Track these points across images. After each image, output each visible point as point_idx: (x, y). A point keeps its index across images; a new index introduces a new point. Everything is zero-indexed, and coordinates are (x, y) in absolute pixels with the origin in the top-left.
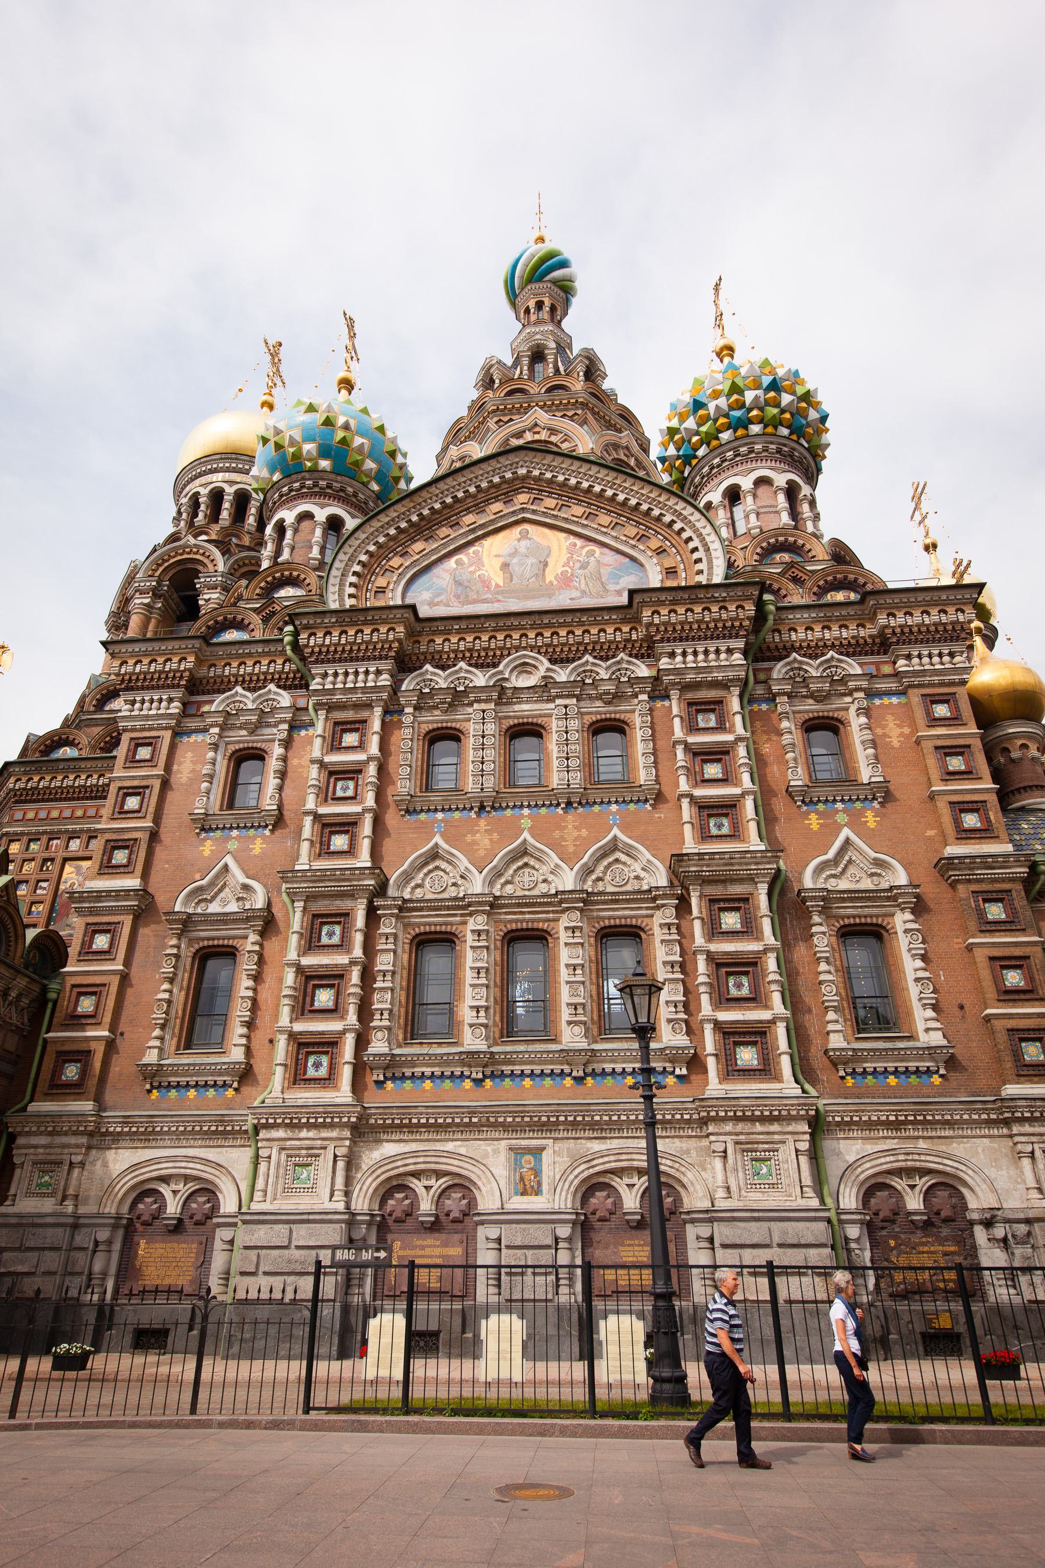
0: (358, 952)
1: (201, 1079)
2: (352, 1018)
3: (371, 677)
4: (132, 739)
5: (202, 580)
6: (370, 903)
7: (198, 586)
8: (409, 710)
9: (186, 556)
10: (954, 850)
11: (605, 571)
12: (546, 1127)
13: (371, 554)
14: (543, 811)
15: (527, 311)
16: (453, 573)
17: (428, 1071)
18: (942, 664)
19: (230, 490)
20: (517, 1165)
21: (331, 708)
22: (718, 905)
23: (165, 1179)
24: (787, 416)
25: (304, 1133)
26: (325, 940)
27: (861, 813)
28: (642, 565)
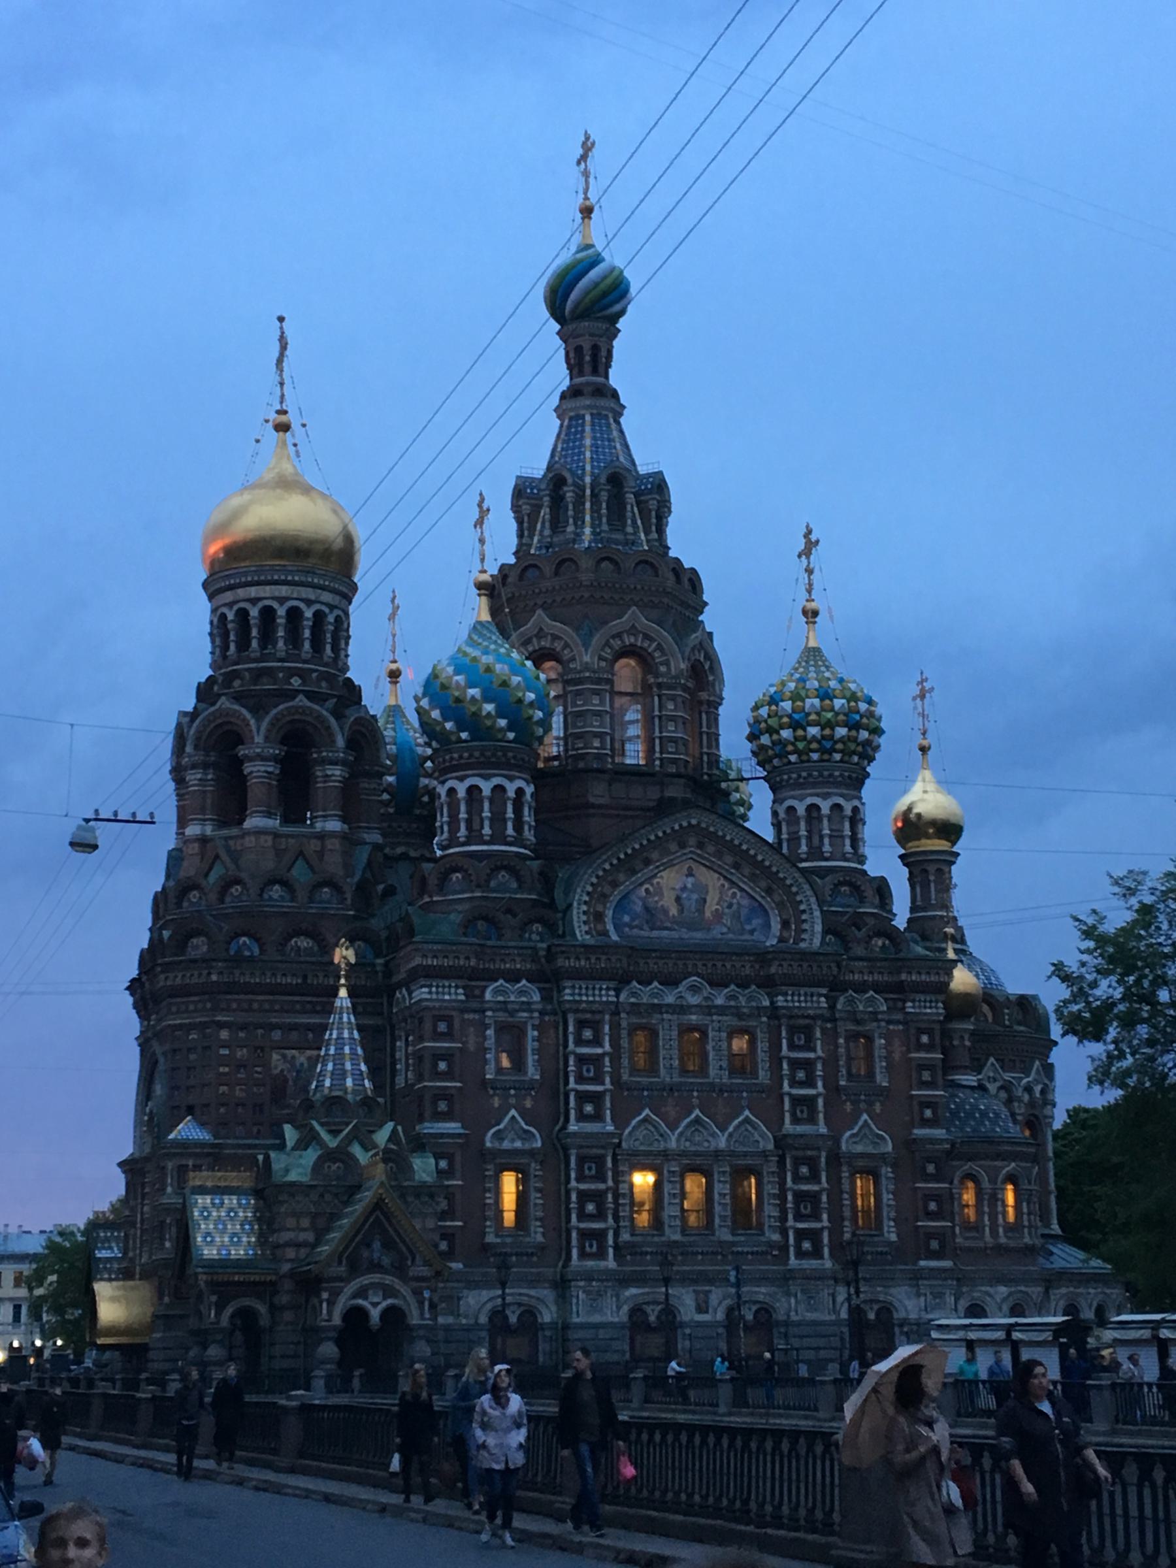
0: (610, 1183)
3: (603, 992)
4: (434, 1016)
5: (324, 754)
8: (623, 1015)
9: (296, 717)
10: (919, 1132)
12: (711, 1281)
13: (592, 884)
15: (579, 350)
16: (643, 900)
17: (649, 1250)
18: (930, 1007)
21: (577, 1011)
22: (797, 1162)
24: (860, 749)
25: (594, 1283)
26: (587, 1172)
28: (766, 911)
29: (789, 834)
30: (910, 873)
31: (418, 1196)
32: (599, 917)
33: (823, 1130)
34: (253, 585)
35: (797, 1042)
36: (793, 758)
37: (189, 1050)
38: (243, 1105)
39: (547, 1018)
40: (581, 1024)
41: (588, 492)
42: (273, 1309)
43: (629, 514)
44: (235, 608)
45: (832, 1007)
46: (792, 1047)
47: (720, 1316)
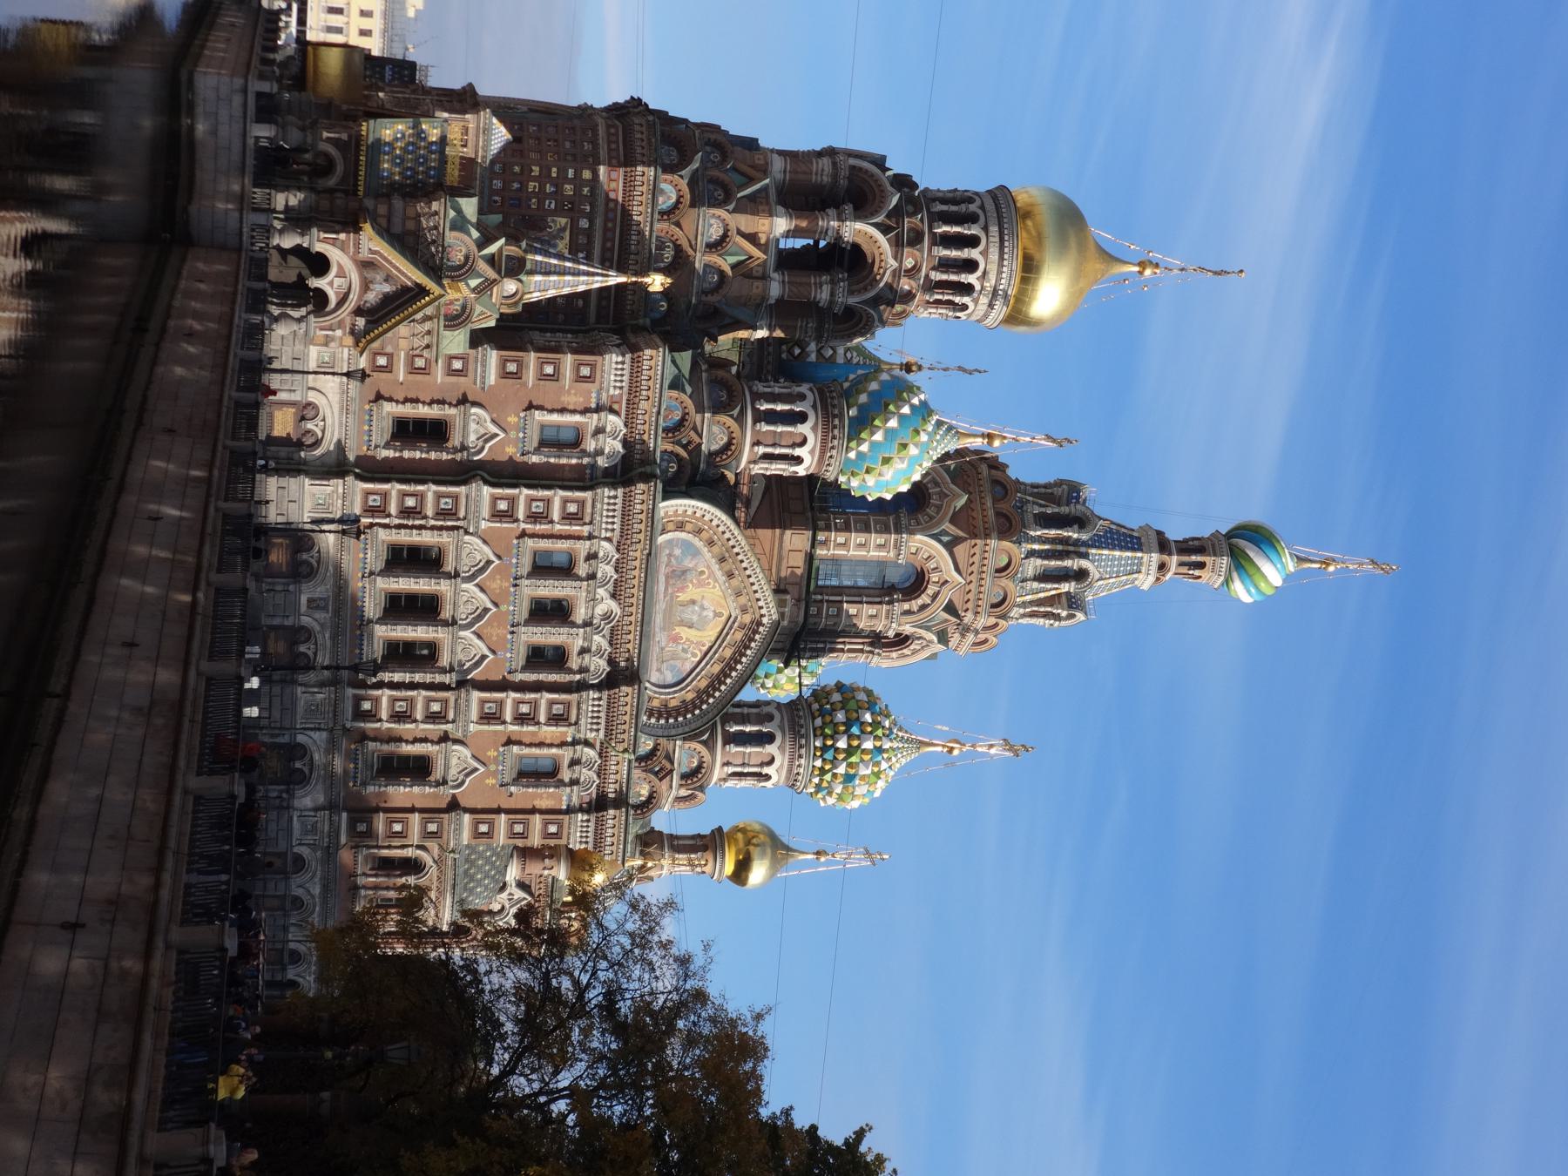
0: (432, 522)
1: (374, 433)
2: (397, 521)
3: (610, 527)
5: (842, 284)
6: (462, 527)
7: (840, 276)
8: (588, 543)
11: (678, 663)
14: (511, 617)
17: (369, 556)
18: (581, 837)
19: (972, 279)
20: (321, 599)
21: (594, 501)
23: (324, 420)
25: (340, 502)
27: (496, 778)
29: (748, 714)
30: (705, 836)
31: (429, 333)
32: (680, 526)
33: (472, 727)
34: (1000, 228)
35: (555, 706)
36: (818, 722)
37: (571, 141)
38: (519, 190)
39: (588, 471)
40: (582, 503)
41: (1071, 548)
42: (331, 191)
43: (1049, 586)
44: (980, 212)
45: (587, 743)
46: (551, 703)
47: (305, 620)
